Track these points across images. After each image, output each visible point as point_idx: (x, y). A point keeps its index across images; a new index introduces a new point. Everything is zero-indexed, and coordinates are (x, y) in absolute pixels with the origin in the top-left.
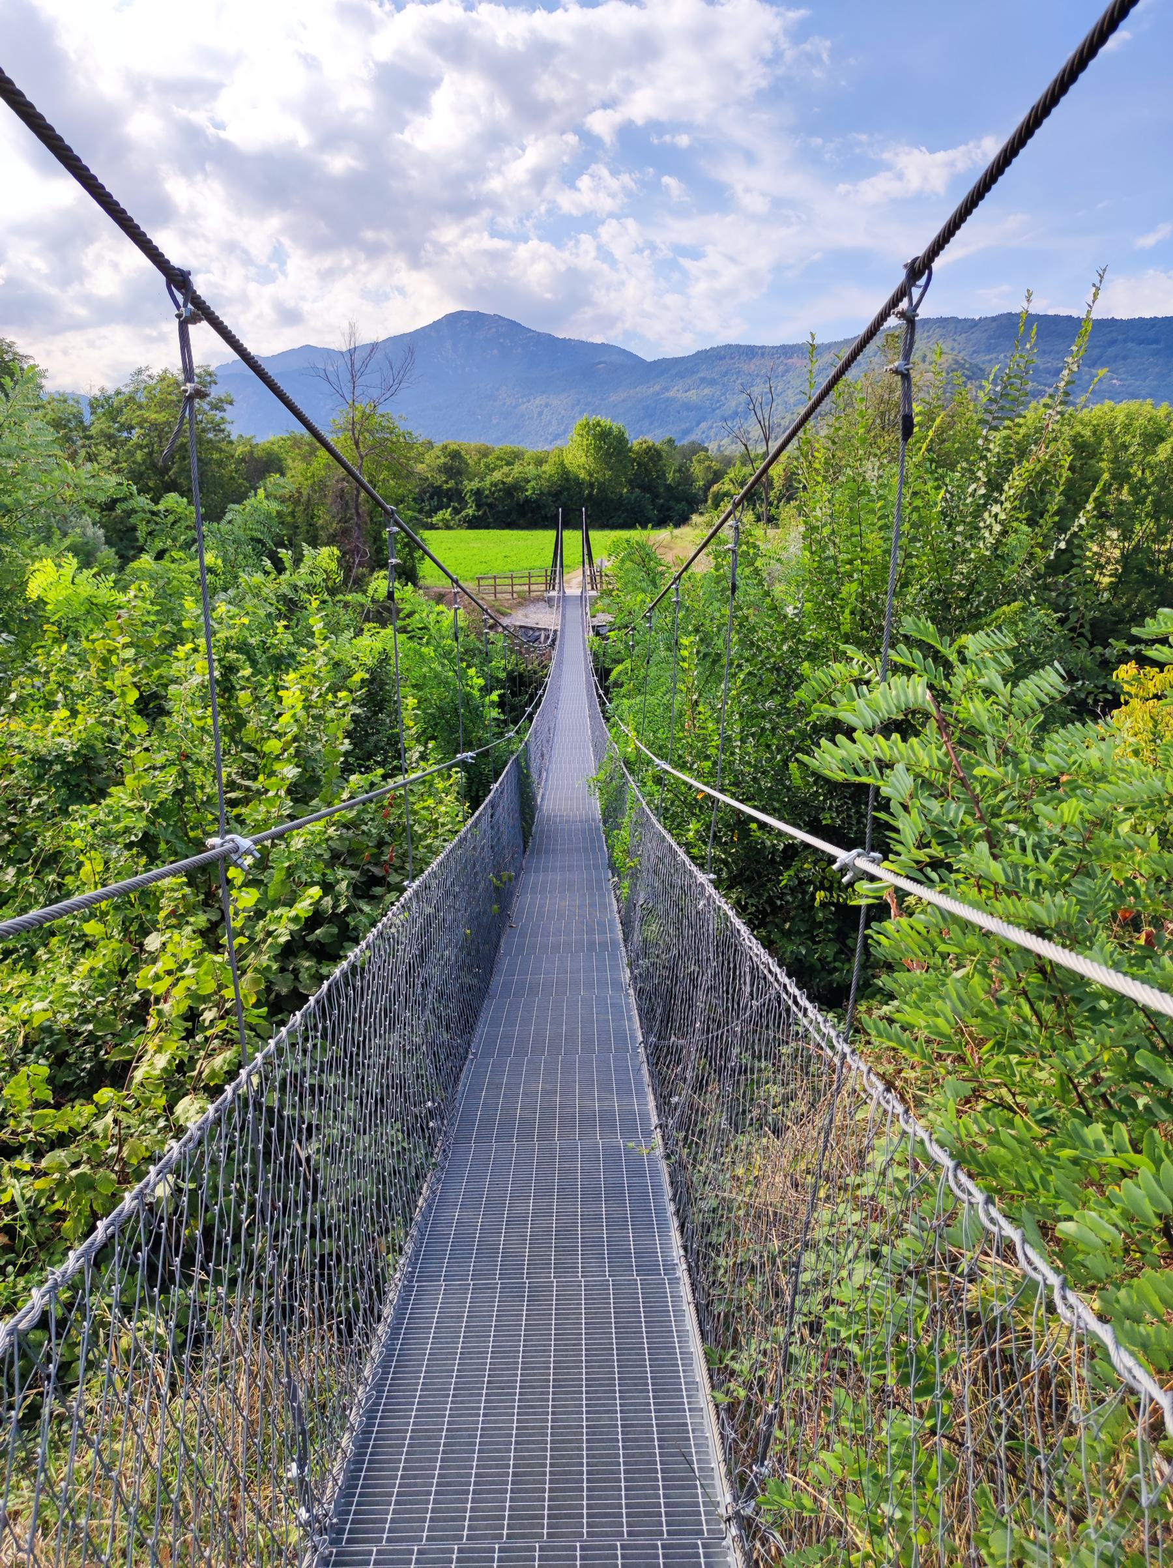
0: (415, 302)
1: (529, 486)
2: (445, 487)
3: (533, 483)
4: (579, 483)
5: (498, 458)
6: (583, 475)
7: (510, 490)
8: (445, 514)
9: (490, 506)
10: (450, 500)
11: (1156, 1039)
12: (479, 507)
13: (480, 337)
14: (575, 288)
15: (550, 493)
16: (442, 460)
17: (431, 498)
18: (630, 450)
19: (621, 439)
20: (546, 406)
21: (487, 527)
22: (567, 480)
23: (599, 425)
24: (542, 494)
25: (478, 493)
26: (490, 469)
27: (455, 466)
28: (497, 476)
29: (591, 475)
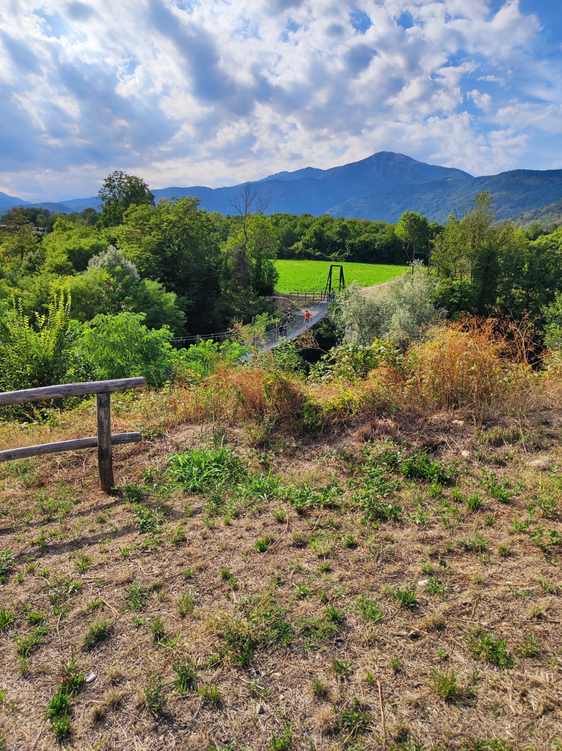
0: (356, 150)
1: (376, 244)
2: (338, 241)
3: (378, 242)
4: (400, 243)
5: (373, 228)
6: (403, 239)
7: (367, 245)
8: (336, 254)
9: (357, 251)
10: (339, 248)
11: (368, 566)
12: (351, 252)
13: (386, 167)
14: (432, 144)
15: (386, 247)
16: (338, 229)
17: (332, 246)
18: (429, 228)
19: (424, 223)
20: (420, 198)
21: (354, 261)
22: (395, 241)
23: (413, 215)
24: (382, 247)
25: (352, 245)
26: (359, 234)
27: (344, 233)
28: (362, 238)
29: (406, 239)
